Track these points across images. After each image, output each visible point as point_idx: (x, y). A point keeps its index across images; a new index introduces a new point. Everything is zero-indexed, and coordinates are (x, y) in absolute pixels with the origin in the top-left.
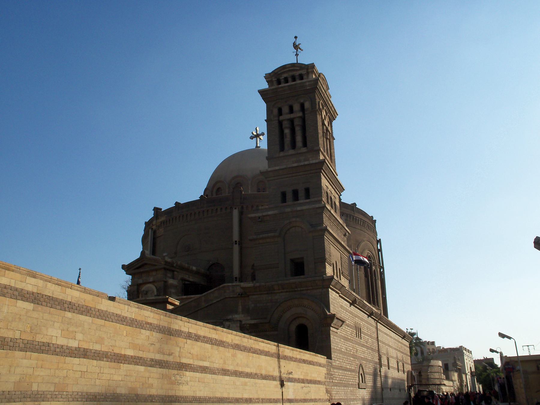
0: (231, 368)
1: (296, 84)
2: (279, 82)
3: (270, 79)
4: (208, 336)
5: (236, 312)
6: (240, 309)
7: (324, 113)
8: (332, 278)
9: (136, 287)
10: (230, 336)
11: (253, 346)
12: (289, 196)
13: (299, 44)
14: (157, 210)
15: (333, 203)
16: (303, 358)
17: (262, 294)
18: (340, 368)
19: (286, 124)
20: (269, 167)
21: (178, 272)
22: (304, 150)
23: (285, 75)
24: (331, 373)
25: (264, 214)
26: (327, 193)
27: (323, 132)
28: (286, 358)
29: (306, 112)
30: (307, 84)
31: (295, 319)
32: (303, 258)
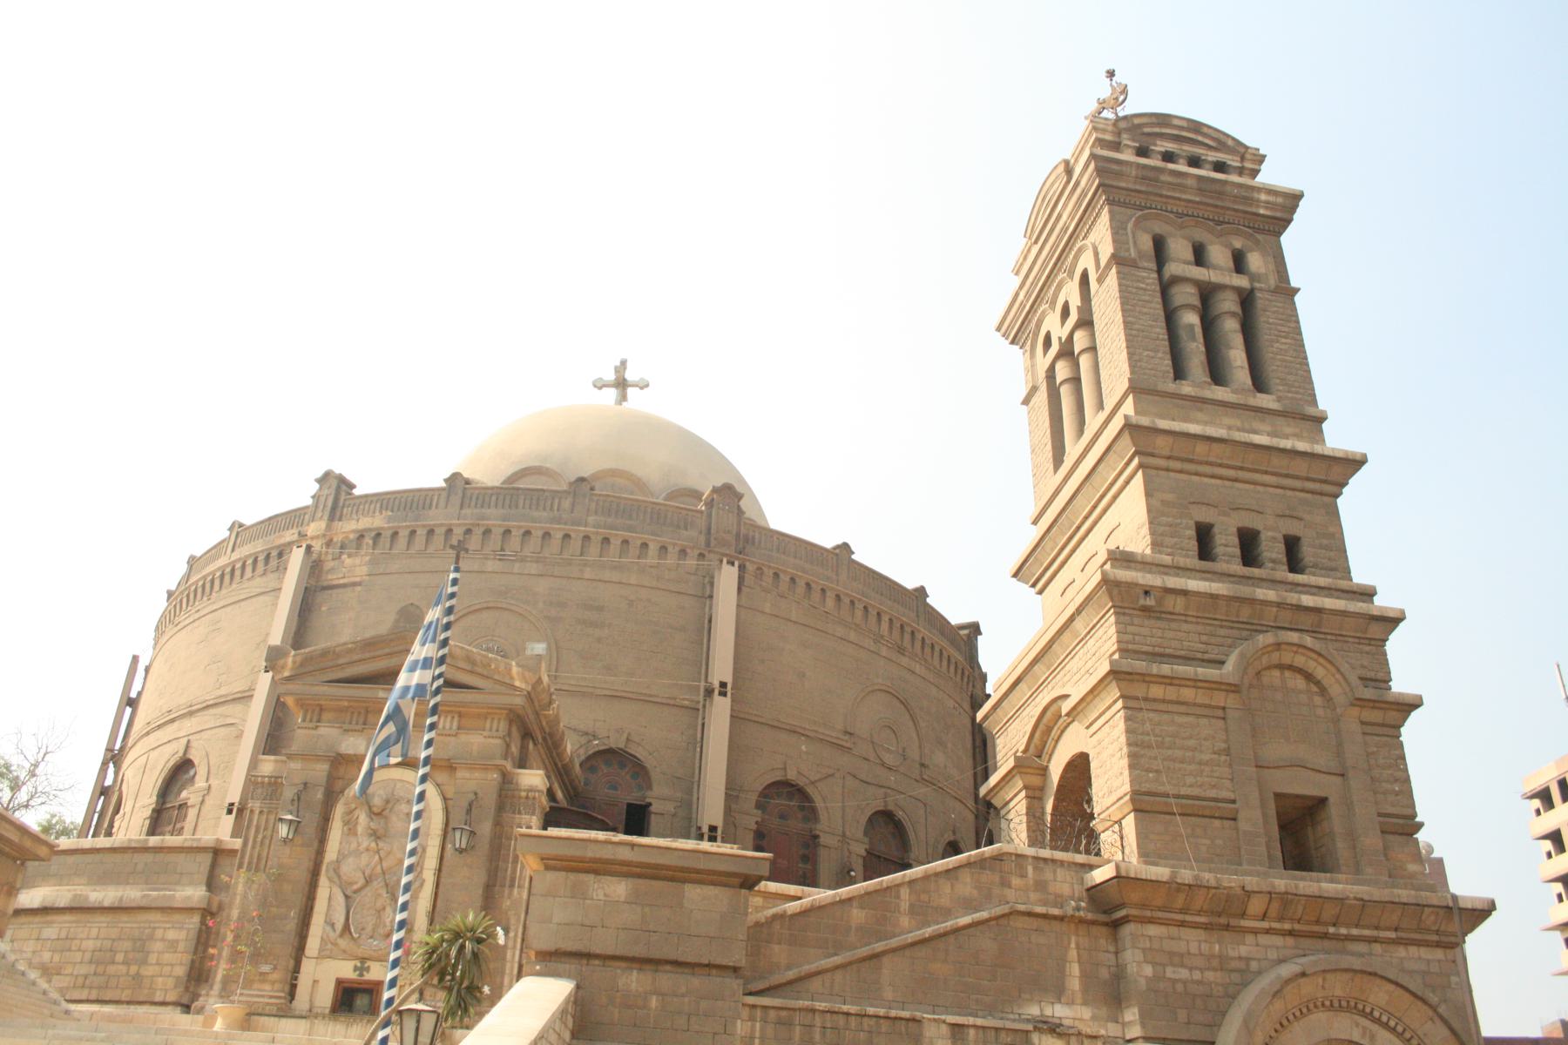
6: (1074, 984)
9: (322, 769)
17: (1182, 924)
19: (1185, 295)
23: (1170, 146)
32: (1323, 801)
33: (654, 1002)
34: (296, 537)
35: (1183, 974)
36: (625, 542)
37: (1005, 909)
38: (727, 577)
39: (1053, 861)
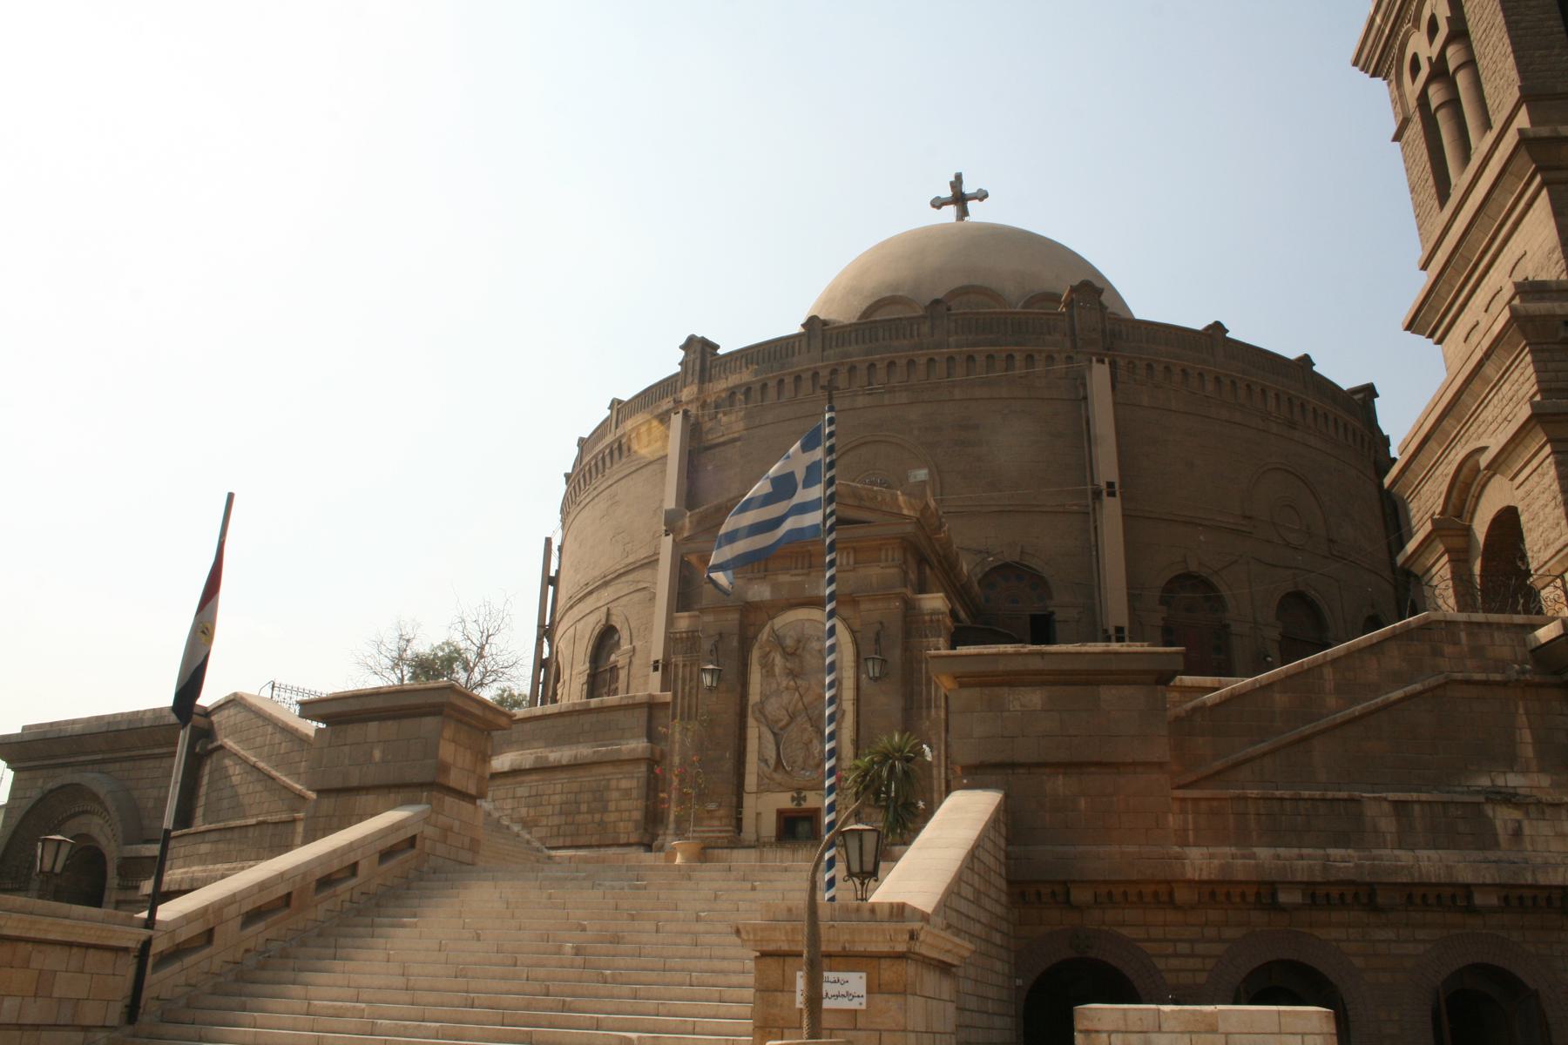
5: (1511, 762)
6: (1528, 751)
9: (733, 617)
33: (1082, 803)
34: (671, 405)
36: (990, 357)
37: (1440, 679)
38: (1099, 377)
39: (1489, 624)
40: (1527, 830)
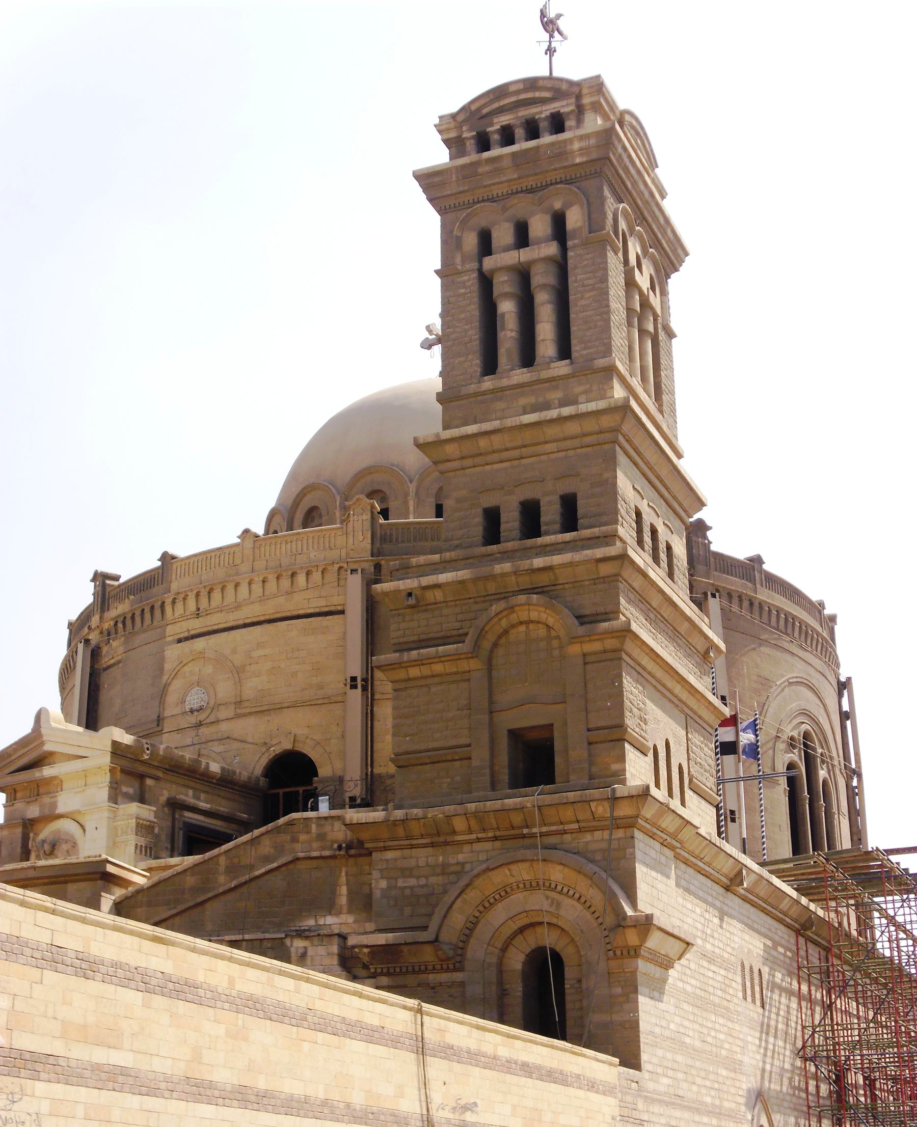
0: (224, 1076)
1: (537, 148)
2: (484, 144)
3: (453, 134)
4: (133, 964)
5: (330, 907)
6: (343, 900)
7: (634, 248)
8: (644, 794)
10: (222, 965)
11: (319, 1005)
12: (511, 521)
13: (559, 16)
14: (101, 579)
15: (662, 547)
16: (523, 1057)
17: (412, 847)
18: (676, 1101)
20: (446, 427)
21: (157, 779)
22: (562, 368)
23: (505, 119)
24: (635, 1114)
25: (426, 581)
26: (638, 514)
27: (629, 310)
28: (450, 1053)
29: (570, 243)
30: (576, 146)
31: (522, 930)
35: (412, 882)
40: (310, 953)
